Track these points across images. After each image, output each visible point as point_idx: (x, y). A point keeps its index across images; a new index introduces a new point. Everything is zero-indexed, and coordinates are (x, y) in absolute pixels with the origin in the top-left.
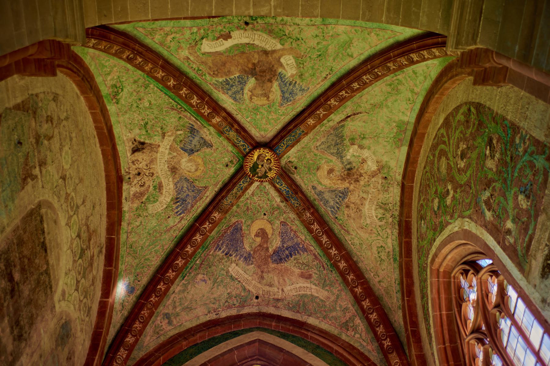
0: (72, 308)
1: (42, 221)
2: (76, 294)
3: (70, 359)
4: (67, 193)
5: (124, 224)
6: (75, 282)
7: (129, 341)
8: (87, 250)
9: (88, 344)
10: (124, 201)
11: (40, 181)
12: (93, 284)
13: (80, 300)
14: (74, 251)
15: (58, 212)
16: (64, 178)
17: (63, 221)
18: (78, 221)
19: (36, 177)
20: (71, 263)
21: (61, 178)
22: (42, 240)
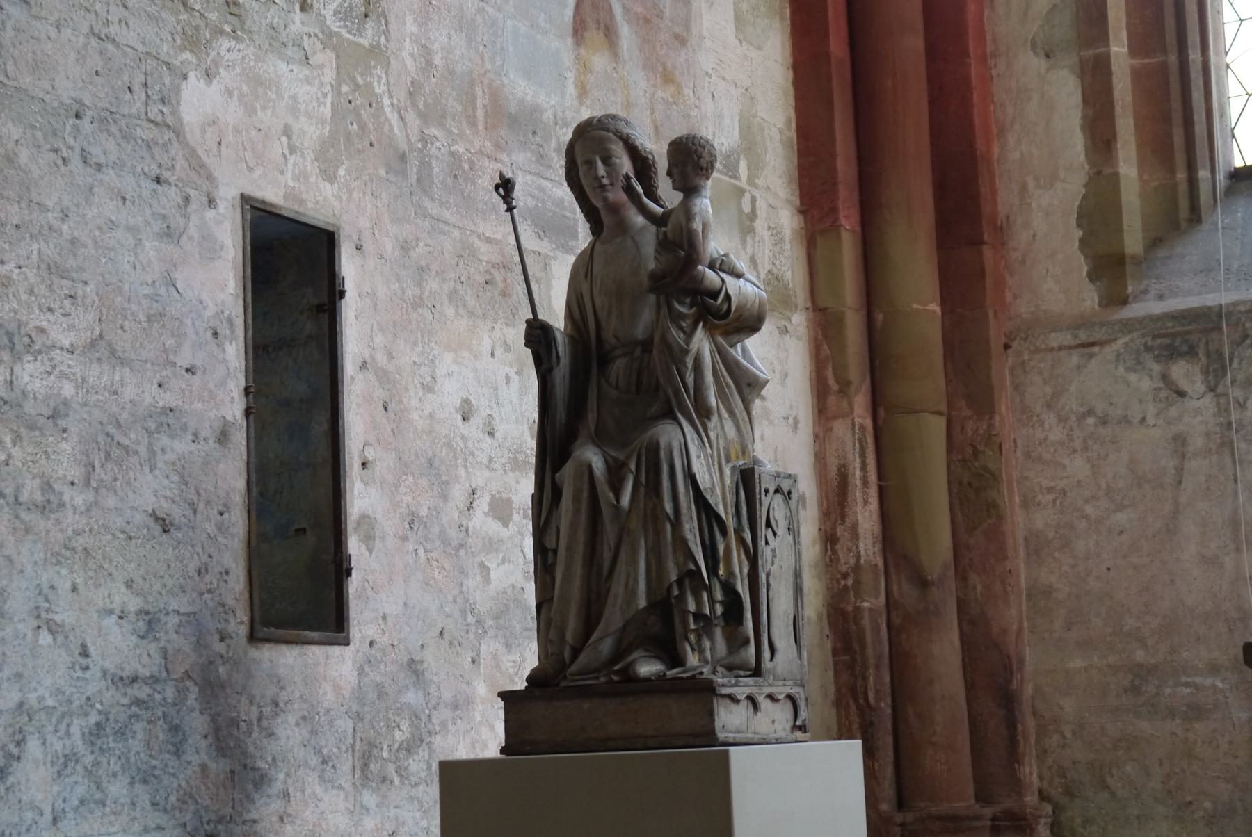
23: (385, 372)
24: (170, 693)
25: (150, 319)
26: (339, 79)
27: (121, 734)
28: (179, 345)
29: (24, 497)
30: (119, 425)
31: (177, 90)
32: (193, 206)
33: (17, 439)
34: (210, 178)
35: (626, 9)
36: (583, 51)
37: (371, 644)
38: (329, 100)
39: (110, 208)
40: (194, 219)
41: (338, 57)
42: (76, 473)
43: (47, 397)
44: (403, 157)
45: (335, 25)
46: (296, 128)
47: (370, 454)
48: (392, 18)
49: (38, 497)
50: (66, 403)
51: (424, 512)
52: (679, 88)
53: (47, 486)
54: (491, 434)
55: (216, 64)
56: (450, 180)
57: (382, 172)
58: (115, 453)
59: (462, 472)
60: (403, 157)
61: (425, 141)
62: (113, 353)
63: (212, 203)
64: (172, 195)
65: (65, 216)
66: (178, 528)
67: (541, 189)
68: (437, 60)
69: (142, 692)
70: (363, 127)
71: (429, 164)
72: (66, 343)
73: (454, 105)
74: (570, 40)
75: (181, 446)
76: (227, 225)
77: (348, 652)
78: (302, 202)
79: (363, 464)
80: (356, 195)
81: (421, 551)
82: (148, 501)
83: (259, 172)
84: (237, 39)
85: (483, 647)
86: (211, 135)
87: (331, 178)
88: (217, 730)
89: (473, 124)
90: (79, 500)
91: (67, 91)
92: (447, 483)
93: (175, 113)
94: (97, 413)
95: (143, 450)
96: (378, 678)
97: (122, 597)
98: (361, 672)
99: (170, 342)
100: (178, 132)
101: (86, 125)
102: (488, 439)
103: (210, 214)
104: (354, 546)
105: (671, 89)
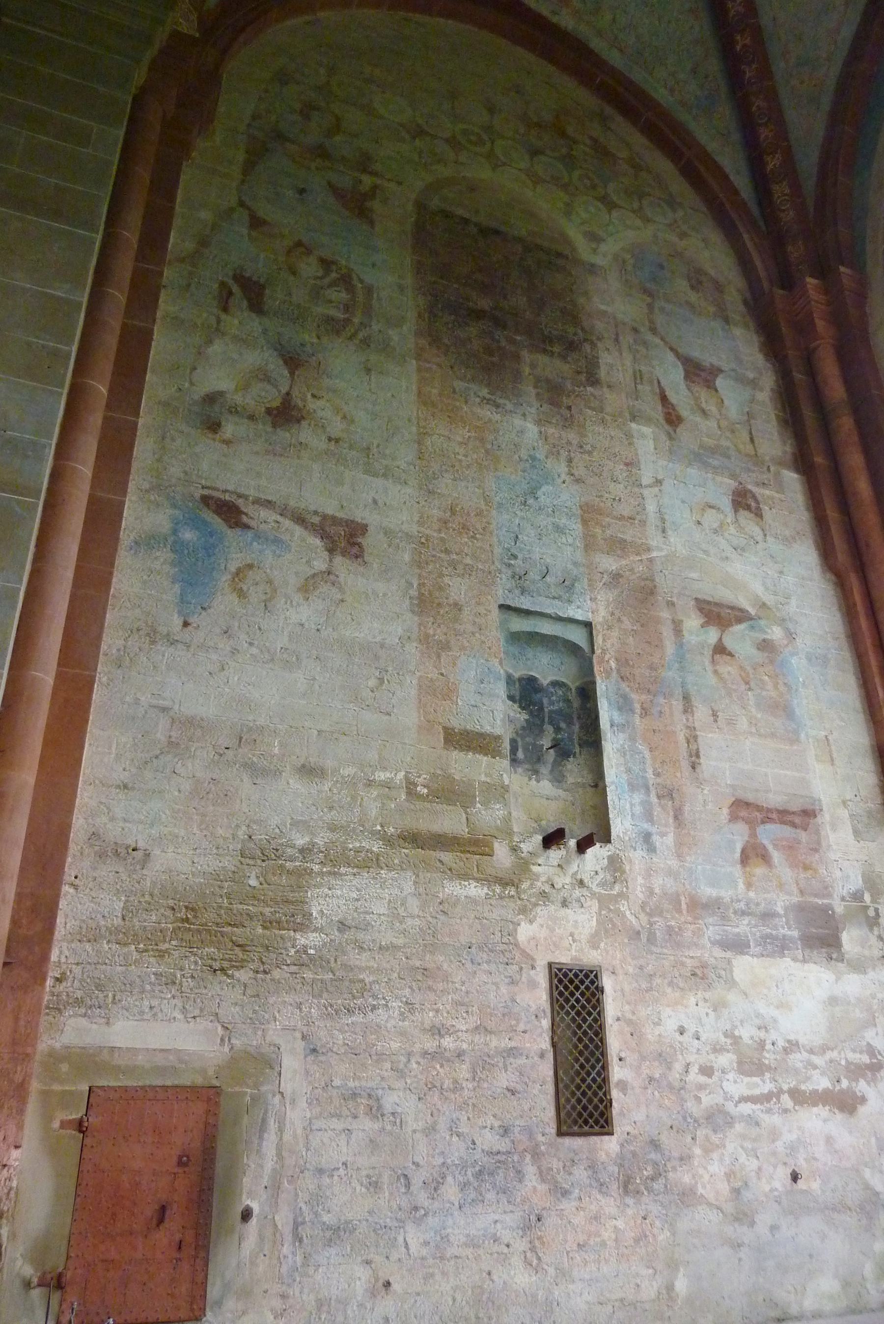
0: (630, 234)
1: (447, 215)
2: (615, 214)
3: (700, 283)
4: (447, 140)
5: (597, 44)
6: (599, 204)
7: (775, 165)
8: (572, 150)
9: (716, 237)
10: (555, 19)
11: (386, 184)
12: (637, 168)
13: (634, 212)
14: (548, 179)
15: (462, 174)
16: (419, 132)
17: (483, 173)
18: (510, 142)
19: (375, 187)
20: (562, 194)
21: (414, 138)
22: (475, 230)
23: (630, 1020)
24: (516, 1158)
25: (504, 1015)
26: (600, 909)
27: (491, 1174)
28: (518, 1023)
29: (445, 1086)
30: (489, 1056)
31: (516, 930)
32: (524, 970)
33: (442, 1066)
34: (533, 959)
35: (775, 846)
36: (748, 869)
37: (628, 1134)
38: (595, 919)
39: (484, 977)
40: (524, 975)
41: (599, 902)
42: (468, 1076)
43: (455, 1051)
44: (638, 933)
45: (597, 890)
46: (576, 932)
47: (623, 1055)
48: (629, 880)
49: (451, 1086)
50: (463, 1051)
51: (657, 1076)
52: (816, 871)
53: (456, 1081)
54: (698, 1039)
55: (535, 917)
56: (667, 937)
57: (626, 941)
58: (487, 1067)
59: (680, 1057)
60: (638, 933)
61: (651, 924)
62: (486, 1030)
63: (533, 967)
64: (515, 968)
65: (463, 983)
66: (519, 1093)
67: (724, 931)
68: (657, 891)
69: (502, 1158)
70: (614, 925)
71: (655, 934)
72: (464, 1029)
73: (666, 906)
74: (739, 866)
75: (522, 1061)
76: (542, 975)
77: (614, 1138)
78: (581, 960)
79: (620, 1060)
80: (611, 952)
81: (656, 1093)
82: (505, 1084)
83: (557, 952)
84: (545, 905)
85: (698, 1133)
86: (533, 943)
87: (595, 947)
88: (541, 1173)
89: (679, 911)
90: (470, 1086)
91: (464, 940)
92: (670, 1063)
93: (515, 938)
94: (478, 1053)
95: (501, 1065)
96: (632, 1148)
97: (490, 1121)
98: (622, 1145)
99: (513, 1022)
100: (517, 945)
101: (473, 950)
102: (697, 1041)
103: (532, 972)
104: (615, 1094)
105: (811, 872)
